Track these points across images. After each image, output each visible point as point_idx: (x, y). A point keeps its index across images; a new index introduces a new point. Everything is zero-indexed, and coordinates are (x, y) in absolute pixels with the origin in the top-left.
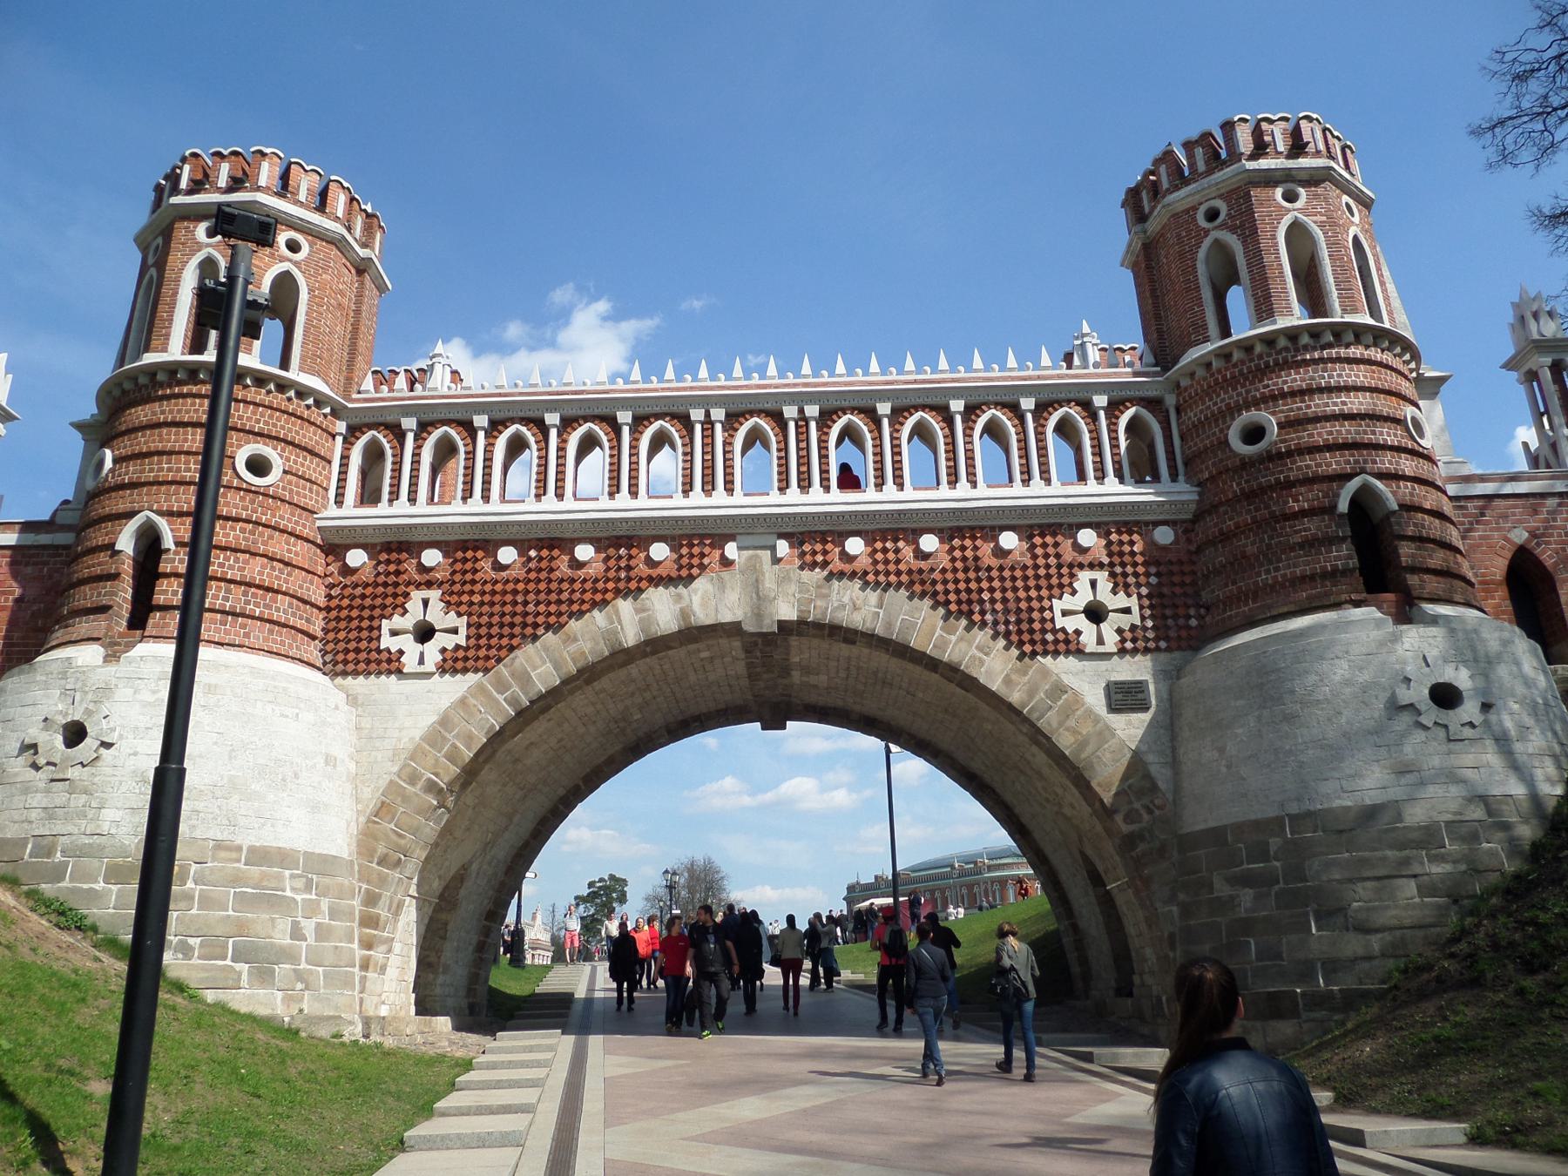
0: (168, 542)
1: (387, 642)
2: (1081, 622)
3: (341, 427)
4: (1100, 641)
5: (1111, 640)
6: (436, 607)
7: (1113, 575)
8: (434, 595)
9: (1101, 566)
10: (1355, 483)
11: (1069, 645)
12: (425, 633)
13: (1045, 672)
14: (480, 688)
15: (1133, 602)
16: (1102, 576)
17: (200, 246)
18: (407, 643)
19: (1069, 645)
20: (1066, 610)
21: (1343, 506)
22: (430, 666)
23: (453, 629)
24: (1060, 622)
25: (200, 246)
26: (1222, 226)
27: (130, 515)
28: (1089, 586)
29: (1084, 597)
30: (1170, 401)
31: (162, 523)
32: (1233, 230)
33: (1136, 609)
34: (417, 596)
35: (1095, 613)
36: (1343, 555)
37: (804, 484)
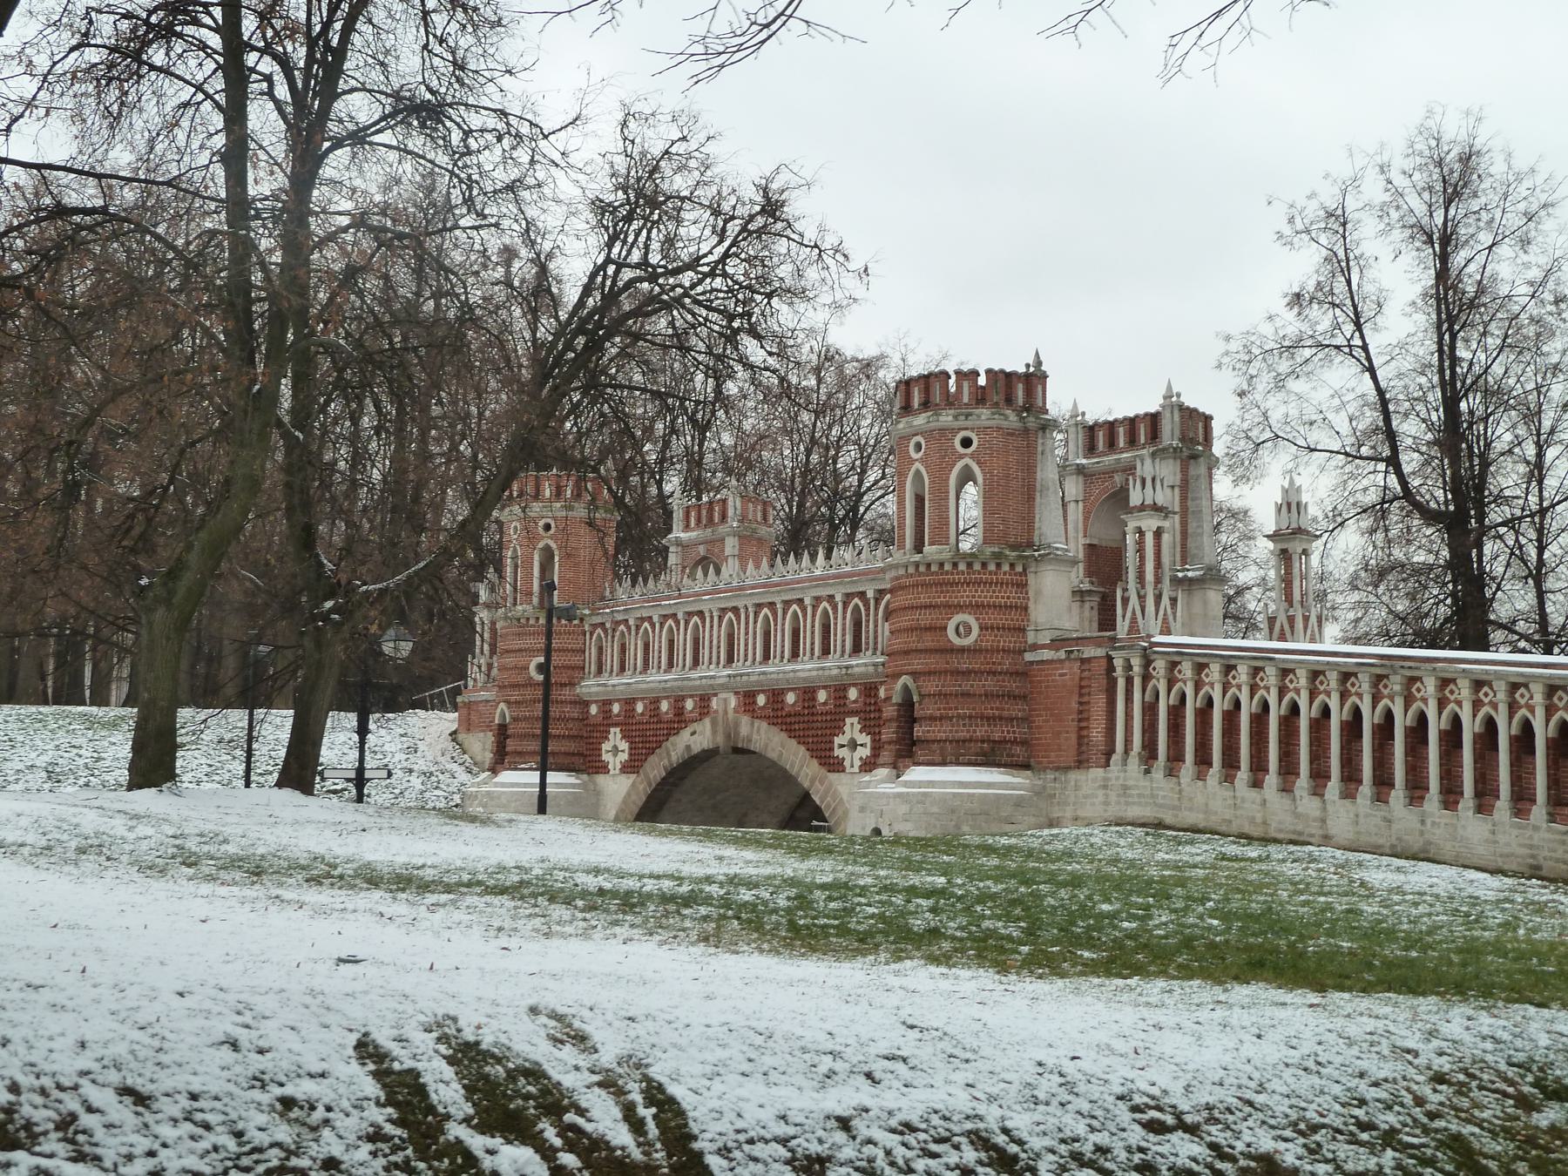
3: (587, 628)
5: (857, 763)
11: (836, 766)
12: (615, 750)
13: (831, 785)
14: (633, 784)
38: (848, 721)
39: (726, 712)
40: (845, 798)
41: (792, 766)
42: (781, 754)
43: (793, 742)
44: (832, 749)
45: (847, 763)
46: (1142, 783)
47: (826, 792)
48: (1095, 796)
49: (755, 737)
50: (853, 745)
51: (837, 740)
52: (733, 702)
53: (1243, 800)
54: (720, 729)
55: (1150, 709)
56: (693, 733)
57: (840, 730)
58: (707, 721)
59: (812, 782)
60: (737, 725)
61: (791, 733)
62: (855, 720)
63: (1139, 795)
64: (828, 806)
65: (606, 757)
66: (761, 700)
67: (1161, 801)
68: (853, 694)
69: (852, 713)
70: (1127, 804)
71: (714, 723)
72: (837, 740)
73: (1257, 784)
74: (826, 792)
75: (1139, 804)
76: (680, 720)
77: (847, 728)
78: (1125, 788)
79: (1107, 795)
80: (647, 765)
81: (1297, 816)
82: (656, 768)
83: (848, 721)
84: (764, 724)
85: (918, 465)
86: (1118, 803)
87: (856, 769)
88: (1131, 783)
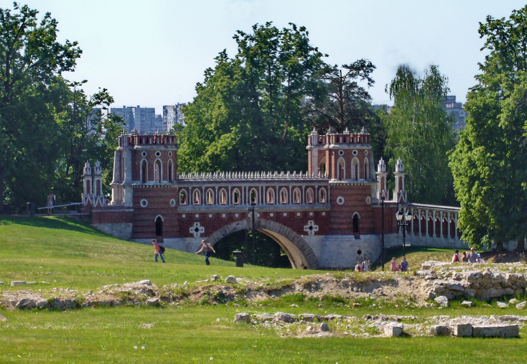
0: (163, 220)
1: (191, 232)
2: (308, 230)
4: (311, 234)
5: (313, 233)
9: (312, 220)
10: (354, 214)
11: (306, 234)
13: (301, 239)
15: (317, 227)
17: (156, 158)
18: (195, 233)
19: (306, 234)
20: (306, 228)
21: (352, 218)
22: (199, 236)
23: (202, 230)
24: (305, 230)
25: (156, 158)
27: (155, 215)
28: (311, 223)
29: (309, 225)
30: (329, 187)
32: (344, 158)
33: (318, 228)
34: (195, 223)
35: (311, 228)
36: (351, 226)
37: (262, 202)
40: (308, 242)
43: (286, 227)
45: (309, 233)
50: (311, 228)
56: (238, 224)
58: (245, 222)
61: (285, 224)
62: (312, 221)
66: (272, 215)
68: (311, 214)
69: (311, 219)
82: (218, 235)
84: (272, 222)
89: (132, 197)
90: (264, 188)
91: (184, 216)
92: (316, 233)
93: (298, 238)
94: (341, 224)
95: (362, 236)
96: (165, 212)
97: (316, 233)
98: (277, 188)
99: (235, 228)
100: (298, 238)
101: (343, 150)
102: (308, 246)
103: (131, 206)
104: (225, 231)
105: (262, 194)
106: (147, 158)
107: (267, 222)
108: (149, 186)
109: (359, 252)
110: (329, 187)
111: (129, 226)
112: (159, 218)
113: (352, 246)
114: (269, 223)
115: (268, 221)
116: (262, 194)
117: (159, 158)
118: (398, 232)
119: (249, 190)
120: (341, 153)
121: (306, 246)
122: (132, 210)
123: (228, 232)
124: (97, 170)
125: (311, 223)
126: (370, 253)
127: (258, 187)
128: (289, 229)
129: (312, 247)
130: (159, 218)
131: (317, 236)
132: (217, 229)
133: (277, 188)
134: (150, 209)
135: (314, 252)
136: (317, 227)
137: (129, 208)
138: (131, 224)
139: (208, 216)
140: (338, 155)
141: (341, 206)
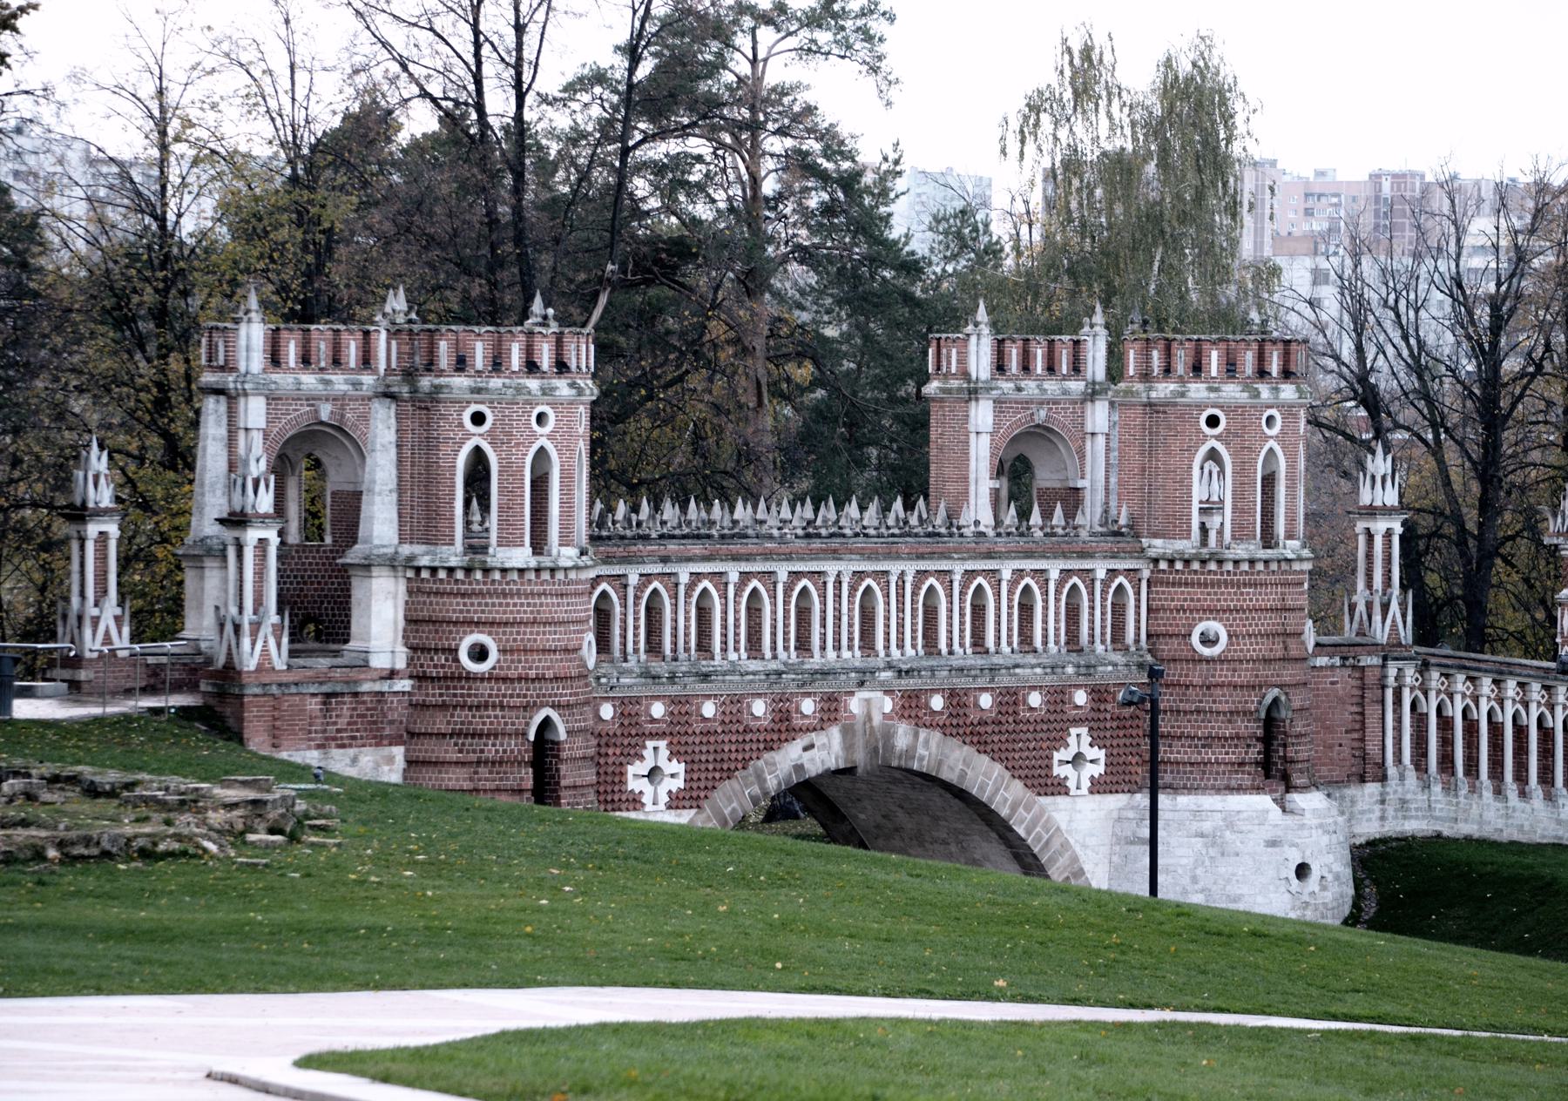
5: (1086, 784)
6: (664, 753)
7: (1091, 729)
8: (662, 744)
11: (1059, 788)
12: (654, 774)
13: (1042, 811)
15: (1101, 754)
16: (1084, 731)
17: (534, 436)
19: (1059, 788)
25: (534, 436)
26: (1218, 438)
29: (1073, 750)
31: (554, 715)
32: (1227, 444)
38: (1074, 731)
39: (869, 718)
40: (1063, 827)
41: (982, 788)
42: (963, 775)
43: (985, 759)
44: (1049, 767)
45: (1071, 784)
46: (1420, 797)
47: (1035, 821)
48: (1371, 811)
49: (921, 751)
50: (1078, 759)
51: (1057, 756)
52: (888, 705)
53: (1514, 810)
54: (860, 742)
55: (1420, 720)
57: (1062, 742)
58: (835, 733)
59: (1014, 808)
60: (888, 736)
61: (982, 746)
62: (1084, 731)
63: (1417, 809)
64: (1038, 838)
65: (633, 785)
66: (937, 703)
67: (1437, 814)
69: (1077, 722)
70: (1405, 818)
71: (847, 732)
72: (1057, 756)
73: (1473, 789)
74: (1035, 821)
75: (1417, 818)
76: (784, 727)
77: (1072, 740)
78: (1403, 802)
79: (1383, 811)
80: (716, 795)
81: (1559, 822)
83: (1074, 731)
84: (936, 736)
85: (1272, 443)
86: (1395, 818)
87: (1085, 790)
88: (1409, 797)
89: (401, 623)
90: (909, 579)
91: (607, 711)
92: (1099, 787)
93: (1028, 809)
94: (1209, 741)
95: (1298, 799)
96: (565, 694)
97: (1099, 787)
98: (957, 578)
99: (799, 768)
100: (1028, 809)
101: (1221, 407)
102: (1065, 845)
103: (401, 664)
104: (761, 779)
105: (901, 610)
106: (491, 436)
107: (916, 735)
108: (504, 571)
109: (1302, 871)
110: (1146, 574)
111: (390, 760)
112: (546, 723)
113: (1273, 843)
114: (927, 742)
115: (923, 733)
116: (901, 610)
117: (550, 437)
118: (1383, 778)
119: (853, 589)
120: (1213, 421)
121: (1056, 845)
122: (404, 685)
123: (772, 783)
124: (256, 492)
125: (1079, 738)
126: (1337, 877)
127: (886, 573)
128: (998, 768)
129: (1078, 849)
130: (546, 723)
131: (1097, 797)
132: (729, 774)
133: (957, 578)
134: (505, 679)
135: (1086, 868)
136: (1101, 754)
137: (392, 674)
138: (399, 752)
139: (699, 708)
140: (1199, 431)
141: (1208, 661)
